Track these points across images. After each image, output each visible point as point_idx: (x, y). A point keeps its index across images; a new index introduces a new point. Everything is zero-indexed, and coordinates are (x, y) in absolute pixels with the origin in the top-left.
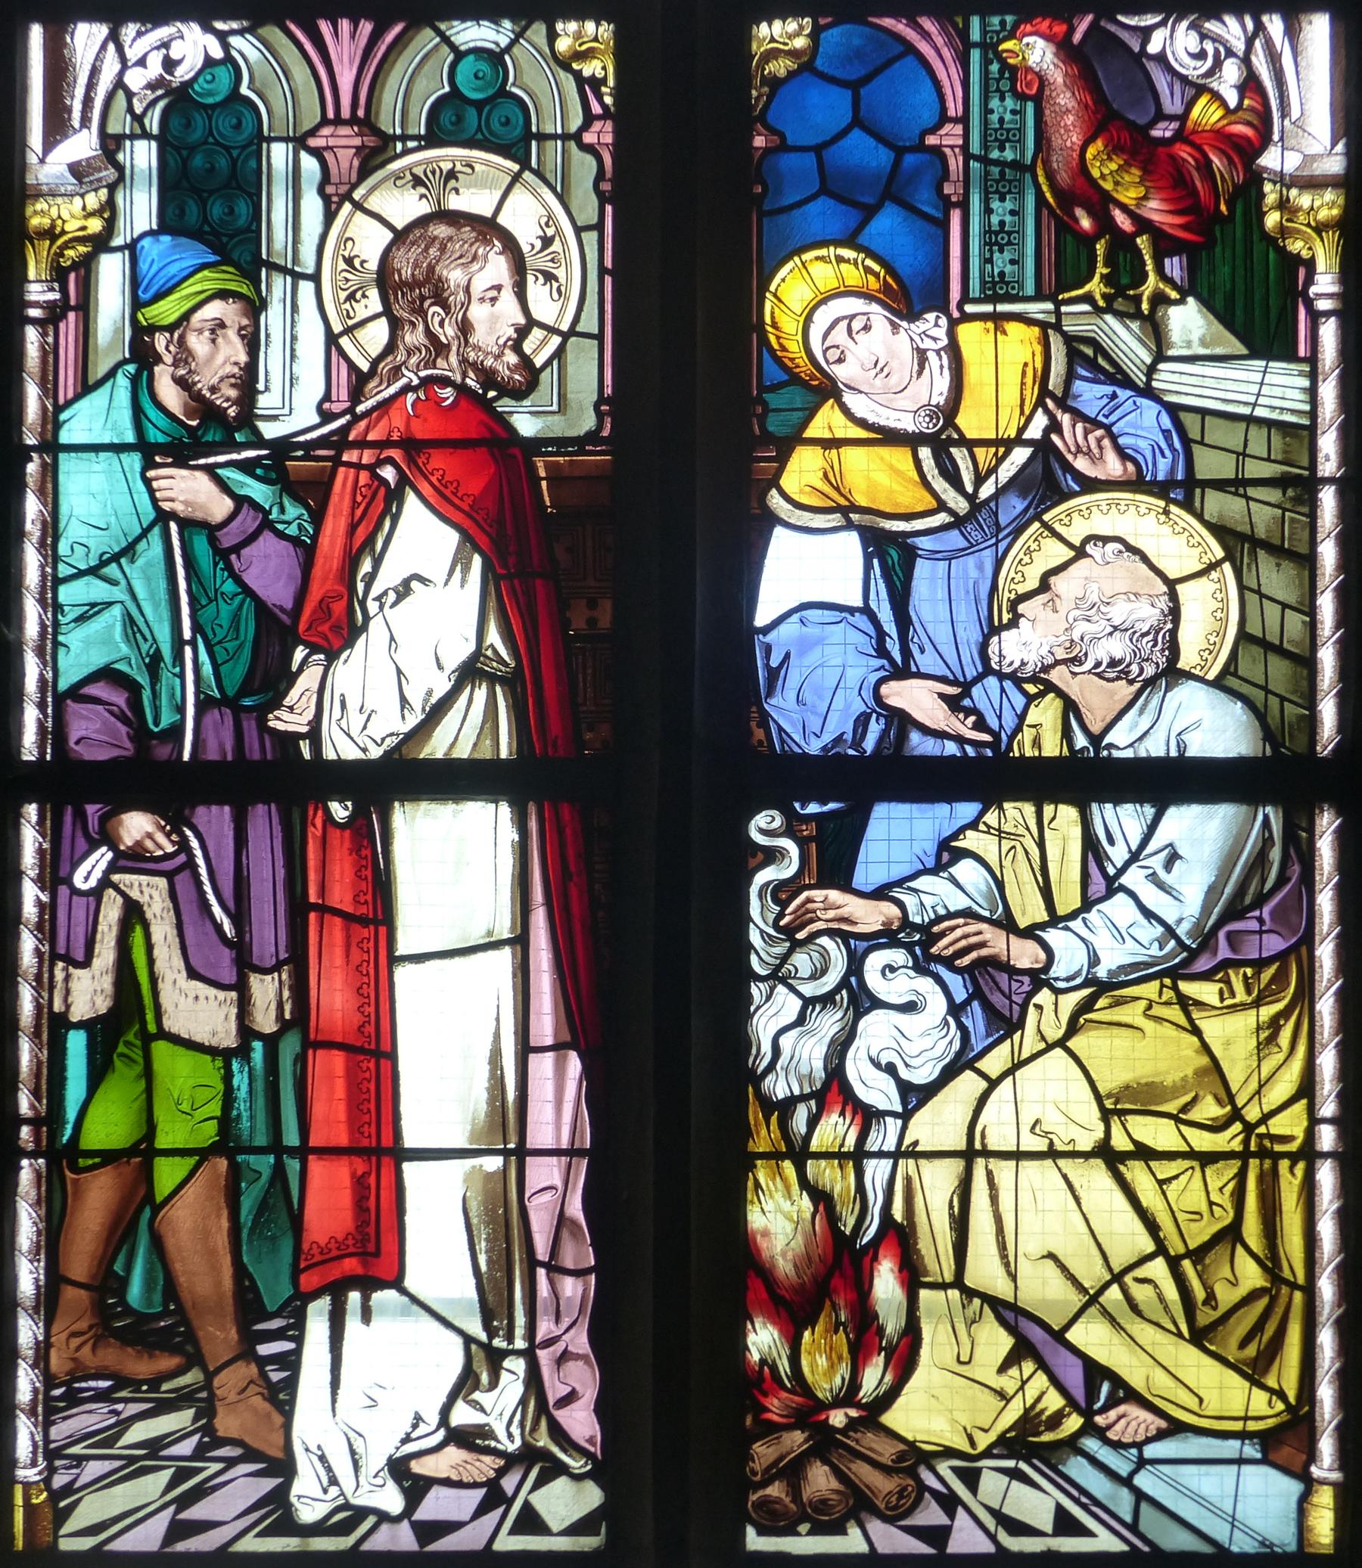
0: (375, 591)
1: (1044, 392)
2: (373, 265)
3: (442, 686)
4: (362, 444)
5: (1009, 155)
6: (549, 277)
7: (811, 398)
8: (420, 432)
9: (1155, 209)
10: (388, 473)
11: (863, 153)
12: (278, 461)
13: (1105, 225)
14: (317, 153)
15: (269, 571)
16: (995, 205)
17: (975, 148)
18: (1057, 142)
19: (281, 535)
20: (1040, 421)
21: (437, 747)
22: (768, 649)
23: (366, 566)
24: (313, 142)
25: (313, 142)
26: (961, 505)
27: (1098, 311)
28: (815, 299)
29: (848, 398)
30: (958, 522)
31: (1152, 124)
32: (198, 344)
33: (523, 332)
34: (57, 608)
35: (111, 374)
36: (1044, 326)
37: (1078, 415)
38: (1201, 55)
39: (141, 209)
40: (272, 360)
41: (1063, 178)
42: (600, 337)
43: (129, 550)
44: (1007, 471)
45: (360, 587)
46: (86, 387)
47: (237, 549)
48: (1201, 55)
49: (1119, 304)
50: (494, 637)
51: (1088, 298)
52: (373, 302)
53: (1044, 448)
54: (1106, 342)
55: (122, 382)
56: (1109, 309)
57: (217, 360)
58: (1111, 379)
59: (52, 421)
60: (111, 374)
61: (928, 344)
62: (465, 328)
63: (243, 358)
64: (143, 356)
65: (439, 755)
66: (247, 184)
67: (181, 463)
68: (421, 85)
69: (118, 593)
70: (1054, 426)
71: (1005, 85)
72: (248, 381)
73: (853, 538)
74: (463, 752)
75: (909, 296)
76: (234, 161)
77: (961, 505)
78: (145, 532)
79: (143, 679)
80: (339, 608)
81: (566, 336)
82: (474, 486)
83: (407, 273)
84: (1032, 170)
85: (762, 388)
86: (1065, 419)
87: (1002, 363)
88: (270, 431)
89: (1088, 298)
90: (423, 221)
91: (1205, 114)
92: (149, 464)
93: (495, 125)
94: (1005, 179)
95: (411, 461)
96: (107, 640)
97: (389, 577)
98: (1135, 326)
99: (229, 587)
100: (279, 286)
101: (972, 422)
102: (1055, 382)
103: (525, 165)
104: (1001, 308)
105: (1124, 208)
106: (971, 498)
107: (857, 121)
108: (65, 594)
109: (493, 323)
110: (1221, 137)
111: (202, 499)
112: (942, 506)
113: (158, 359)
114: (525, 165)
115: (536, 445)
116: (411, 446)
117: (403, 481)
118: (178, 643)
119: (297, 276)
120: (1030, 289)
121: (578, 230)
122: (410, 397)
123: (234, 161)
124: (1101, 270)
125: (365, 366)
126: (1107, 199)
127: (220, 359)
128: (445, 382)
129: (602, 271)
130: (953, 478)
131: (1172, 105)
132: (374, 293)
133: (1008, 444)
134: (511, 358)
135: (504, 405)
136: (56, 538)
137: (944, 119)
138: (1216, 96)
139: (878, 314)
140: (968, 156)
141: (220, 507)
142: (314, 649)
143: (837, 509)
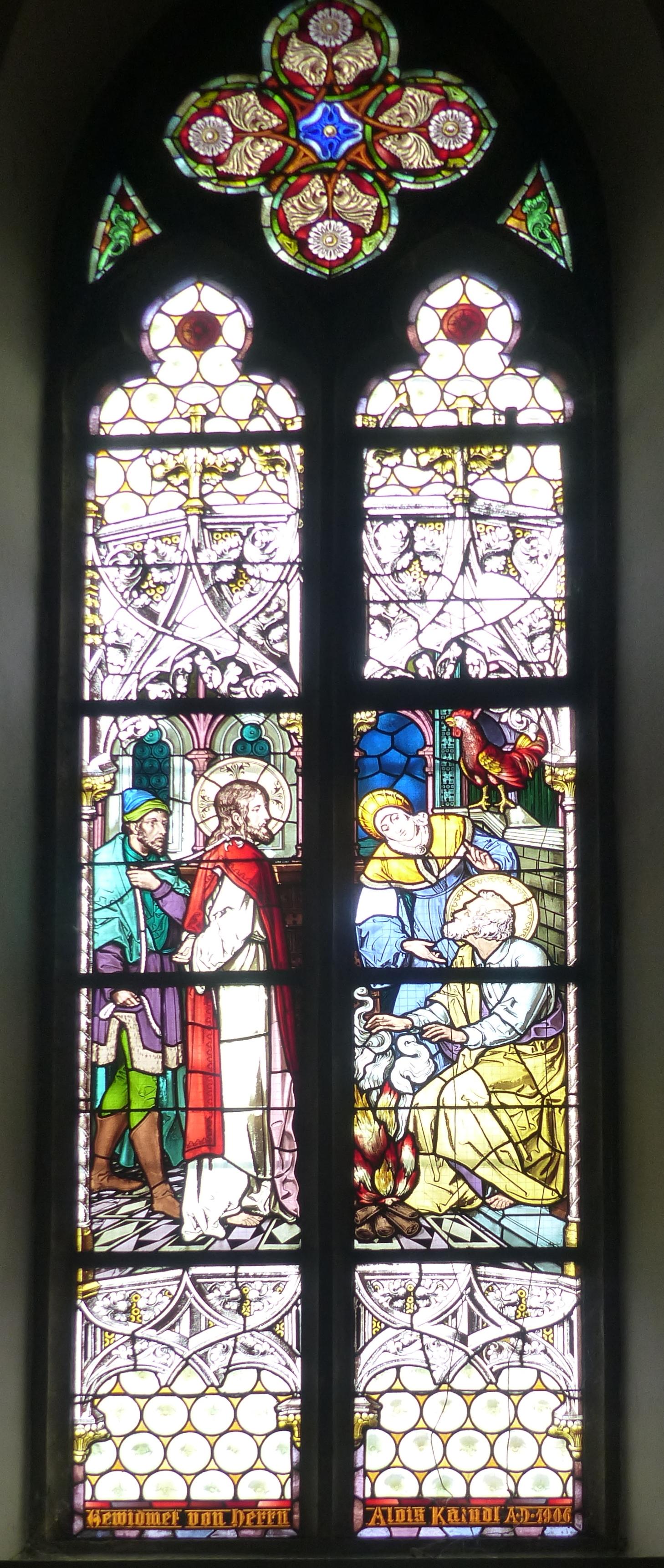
0: (213, 912)
1: (464, 840)
2: (212, 799)
3: (239, 945)
4: (208, 861)
5: (450, 758)
6: (278, 802)
7: (377, 843)
8: (230, 857)
9: (505, 776)
10: (218, 871)
11: (396, 757)
12: (177, 868)
13: (486, 781)
14: (191, 760)
15: (173, 906)
16: (445, 775)
17: (437, 755)
18: (468, 753)
19: (178, 893)
20: (462, 850)
21: (236, 967)
22: (361, 931)
23: (210, 903)
24: (189, 757)
25: (189, 757)
26: (434, 880)
27: (484, 811)
28: (377, 808)
29: (390, 843)
30: (432, 886)
31: (503, 746)
32: (147, 827)
33: (268, 821)
34: (94, 920)
35: (114, 838)
36: (464, 817)
37: (476, 848)
38: (522, 722)
39: (125, 780)
40: (174, 833)
41: (470, 766)
42: (297, 823)
43: (121, 900)
44: (450, 868)
45: (207, 911)
46: (105, 842)
47: (161, 898)
48: (522, 722)
49: (492, 809)
50: (258, 928)
51: (480, 807)
52: (212, 811)
53: (464, 859)
54: (485, 821)
55: (119, 841)
56: (488, 811)
57: (154, 833)
58: (489, 835)
59: (92, 854)
60: (114, 838)
61: (419, 824)
62: (247, 820)
63: (164, 832)
64: (126, 831)
65: (237, 969)
66: (164, 772)
67: (140, 868)
68: (230, 736)
69: (117, 914)
70: (468, 852)
71: (448, 734)
72: (165, 840)
73: (393, 891)
74: (246, 968)
75: (413, 807)
76: (160, 764)
77: (434, 880)
78: (127, 893)
79: (126, 944)
80: (199, 918)
81: (284, 823)
82: (251, 875)
83: (225, 801)
84: (459, 763)
85: (358, 840)
86: (472, 849)
87: (448, 832)
88: (173, 857)
89: (480, 807)
90: (231, 783)
91: (523, 742)
92: (128, 869)
93: (258, 750)
94: (449, 766)
95: (227, 867)
96: (113, 931)
97: (218, 907)
98: (498, 816)
99: (159, 911)
100: (178, 806)
101: (436, 850)
102: (468, 836)
103: (269, 763)
104: (447, 811)
105: (493, 776)
106: (437, 877)
107: (393, 747)
108: (97, 915)
109: (257, 820)
110: (530, 751)
111: (148, 881)
112: (426, 880)
113: (132, 832)
114: (269, 763)
115: (273, 861)
116: (227, 862)
117: (223, 874)
118: (139, 931)
119: (184, 803)
120: (458, 805)
121: (289, 786)
122: (226, 845)
123: (160, 764)
124: (485, 797)
125: (209, 834)
126: (487, 772)
127: (155, 832)
128: (239, 839)
129: (298, 800)
130: (430, 871)
131: (511, 739)
132: (213, 809)
133: (451, 858)
134: (264, 830)
135: (261, 847)
136: (94, 895)
137: (425, 745)
138: (527, 736)
139: (401, 813)
140: (435, 758)
141: (155, 884)
142: (190, 933)
143: (387, 881)
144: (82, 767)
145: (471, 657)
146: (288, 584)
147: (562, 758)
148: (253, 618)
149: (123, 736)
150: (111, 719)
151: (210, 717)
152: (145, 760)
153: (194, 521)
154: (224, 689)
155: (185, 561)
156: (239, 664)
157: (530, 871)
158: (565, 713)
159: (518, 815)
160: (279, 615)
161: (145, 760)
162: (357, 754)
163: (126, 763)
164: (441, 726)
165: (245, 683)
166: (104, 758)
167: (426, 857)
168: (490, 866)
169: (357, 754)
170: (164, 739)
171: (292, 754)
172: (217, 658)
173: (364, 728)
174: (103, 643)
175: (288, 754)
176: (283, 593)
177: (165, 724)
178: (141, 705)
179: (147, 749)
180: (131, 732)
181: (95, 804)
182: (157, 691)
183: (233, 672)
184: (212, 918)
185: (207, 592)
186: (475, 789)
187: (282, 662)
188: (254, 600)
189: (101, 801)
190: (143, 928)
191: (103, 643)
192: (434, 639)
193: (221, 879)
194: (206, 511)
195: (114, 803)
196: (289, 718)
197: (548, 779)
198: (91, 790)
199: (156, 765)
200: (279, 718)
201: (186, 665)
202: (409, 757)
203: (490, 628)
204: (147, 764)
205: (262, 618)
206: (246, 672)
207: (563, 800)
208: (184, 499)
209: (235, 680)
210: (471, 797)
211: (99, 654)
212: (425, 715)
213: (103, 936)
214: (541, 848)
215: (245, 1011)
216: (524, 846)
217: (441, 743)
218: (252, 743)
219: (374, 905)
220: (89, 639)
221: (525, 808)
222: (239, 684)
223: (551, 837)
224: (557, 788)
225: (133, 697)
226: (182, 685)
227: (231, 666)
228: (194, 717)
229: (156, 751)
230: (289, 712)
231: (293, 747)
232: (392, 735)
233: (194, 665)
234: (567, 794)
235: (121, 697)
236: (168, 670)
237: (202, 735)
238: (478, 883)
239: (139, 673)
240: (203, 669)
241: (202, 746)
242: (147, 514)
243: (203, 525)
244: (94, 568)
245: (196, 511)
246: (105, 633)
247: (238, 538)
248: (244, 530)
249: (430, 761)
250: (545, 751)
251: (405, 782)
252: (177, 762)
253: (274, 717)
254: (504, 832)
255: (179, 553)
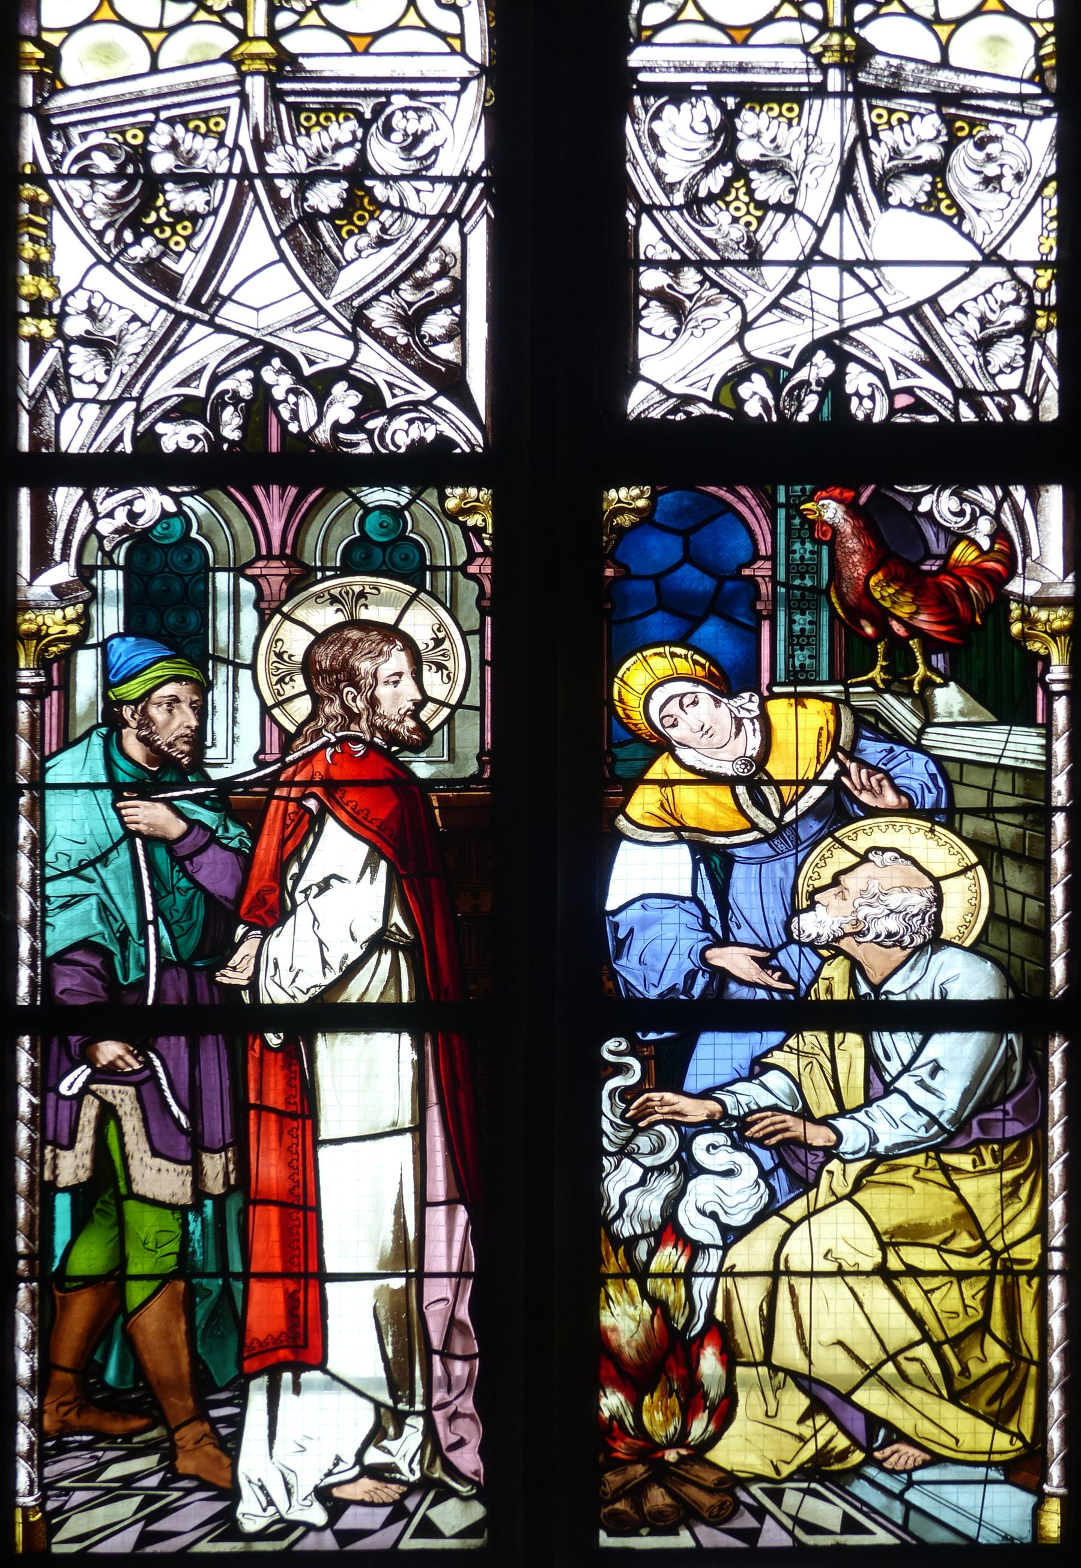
0: (302, 886)
1: (836, 747)
2: (299, 658)
3: (355, 952)
4: (290, 783)
5: (808, 582)
6: (440, 667)
7: (650, 751)
8: (337, 774)
9: (923, 621)
10: (312, 804)
11: (691, 579)
12: (223, 795)
13: (884, 631)
14: (252, 579)
15: (215, 872)
16: (797, 617)
17: (782, 576)
18: (846, 573)
19: (226, 847)
20: (832, 768)
21: (353, 993)
22: (616, 927)
23: (294, 869)
24: (249, 572)
25: (249, 572)
26: (770, 826)
27: (879, 692)
28: (651, 682)
29: (680, 752)
30: (767, 838)
31: (922, 561)
32: (158, 714)
33: (419, 705)
34: (45, 899)
35: (88, 734)
36: (835, 702)
37: (862, 764)
38: (961, 513)
39: (110, 619)
40: (218, 725)
41: (851, 598)
42: (481, 709)
43: (103, 858)
44: (804, 804)
45: (290, 883)
46: (66, 743)
47: (190, 857)
48: (961, 513)
49: (895, 687)
50: (397, 918)
51: (871, 682)
52: (299, 683)
53: (835, 787)
54: (885, 712)
55: (96, 740)
56: (888, 690)
57: (173, 724)
58: (888, 739)
59: (39, 768)
60: (88, 734)
61: (743, 714)
62: (373, 702)
63: (194, 723)
64: (112, 720)
65: (354, 1000)
66: (197, 601)
67: (145, 796)
68: (337, 532)
69: (95, 888)
70: (844, 771)
71: (805, 534)
72: (198, 739)
73: (685, 848)
74: (373, 997)
75: (727, 681)
76: (186, 586)
77: (770, 826)
78: (115, 846)
79: (115, 948)
80: (272, 898)
81: (454, 708)
82: (382, 814)
83: (326, 663)
84: (826, 592)
85: (611, 745)
86: (853, 767)
87: (801, 731)
88: (215, 774)
89: (871, 682)
90: (338, 628)
91: (963, 553)
92: (118, 797)
93: (396, 558)
94: (805, 600)
95: (330, 795)
96: (86, 921)
97: (313, 875)
98: (908, 702)
99: (184, 883)
100: (223, 673)
101: (777, 768)
102: (844, 740)
103: (421, 588)
104: (800, 689)
105: (900, 620)
106: (778, 821)
107: (688, 558)
108: (50, 889)
109: (395, 699)
110: (976, 571)
111: (160, 822)
112: (754, 827)
113: (126, 724)
114: (421, 588)
115: (431, 784)
116: (331, 786)
117: (323, 810)
118: (143, 923)
119: (237, 667)
120: (825, 676)
121: (464, 634)
122: (329, 751)
123: (186, 586)
124: (881, 662)
125: (292, 729)
126: (887, 614)
127: (175, 723)
128: (357, 740)
129: (483, 663)
130: (766, 810)
131: (938, 546)
132: (299, 679)
133: (808, 784)
134: (410, 723)
135: (405, 756)
136: (44, 849)
137: (756, 557)
138: (973, 542)
139: (704, 694)
140: (775, 583)
141: (176, 828)
142: (252, 927)
143: (672, 829)
144: (15, 589)
145: (857, 379)
146: (463, 223)
147: (1046, 586)
148: (387, 291)
149: (105, 527)
150: (78, 493)
151: (292, 492)
152: (152, 576)
153: (256, 87)
154: (323, 434)
155: (237, 169)
156: (355, 384)
157: (974, 812)
158: (1054, 497)
159: (949, 699)
160: (442, 286)
161: (152, 576)
162: (609, 572)
163: (112, 581)
164: (789, 518)
165: (370, 425)
166: (63, 573)
167: (754, 778)
168: (890, 799)
169: (609, 572)
170: (194, 534)
171: (472, 569)
172: (307, 371)
173: (625, 520)
174: (59, 333)
175: (463, 568)
176: (451, 239)
177: (195, 505)
178: (144, 464)
179: (157, 556)
180: (121, 517)
181: (43, 664)
182: (175, 437)
183: (343, 403)
184: (299, 897)
185: (285, 234)
186: (858, 648)
187: (451, 381)
188: (388, 255)
189: (57, 658)
190: (150, 916)
191: (59, 333)
192: (773, 340)
193: (316, 824)
194: (283, 66)
195: (87, 663)
196: (463, 497)
197: (1016, 628)
198: (37, 635)
199: (177, 587)
200: (443, 498)
201: (241, 383)
202: (721, 580)
203: (897, 323)
204: (157, 585)
205: (407, 293)
206: (372, 403)
207: (1046, 670)
208: (236, 41)
209: (347, 417)
210: (849, 664)
211: (51, 357)
212: (756, 495)
213: (64, 930)
214: (998, 767)
215: (367, 1080)
216: (962, 762)
217: (789, 551)
218: (383, 546)
219: (645, 872)
220: (28, 327)
221: (965, 686)
222: (356, 426)
223: (1022, 745)
224: (1036, 646)
225: (127, 446)
226: (231, 425)
227: (339, 389)
228: (259, 491)
229: (178, 558)
230: (466, 485)
231: (472, 556)
232: (685, 534)
233: (260, 386)
234: (1055, 660)
235: (101, 445)
236: (201, 392)
237: (276, 527)
238: (865, 835)
239: (139, 400)
240: (278, 393)
241: (276, 551)
242: (154, 70)
243: (275, 96)
244: (39, 179)
245: (259, 65)
246: (63, 315)
247: (353, 124)
248: (367, 107)
249: (765, 589)
250: (1011, 574)
251: (710, 631)
252: (222, 581)
253: (431, 495)
254: (921, 733)
255: (224, 152)
